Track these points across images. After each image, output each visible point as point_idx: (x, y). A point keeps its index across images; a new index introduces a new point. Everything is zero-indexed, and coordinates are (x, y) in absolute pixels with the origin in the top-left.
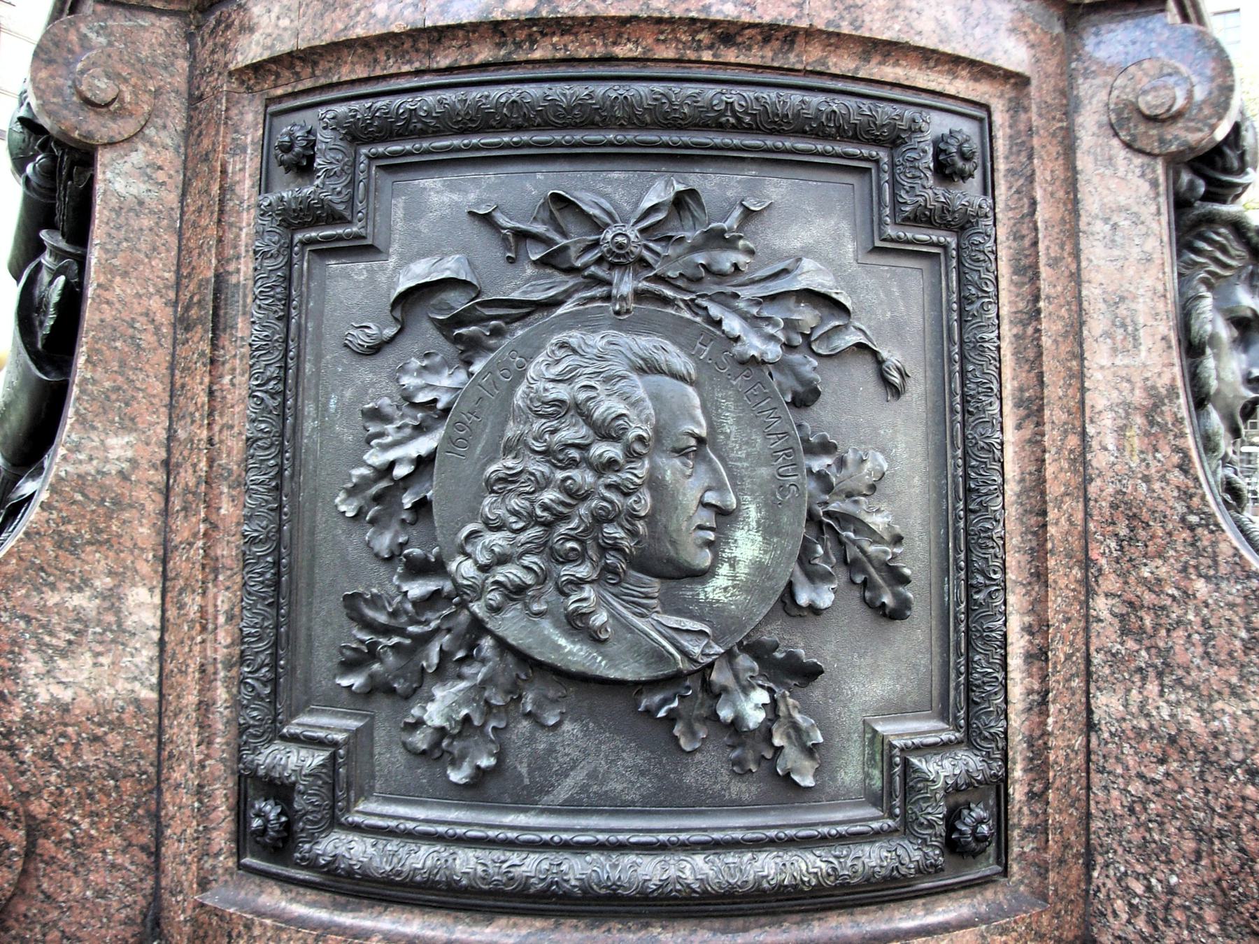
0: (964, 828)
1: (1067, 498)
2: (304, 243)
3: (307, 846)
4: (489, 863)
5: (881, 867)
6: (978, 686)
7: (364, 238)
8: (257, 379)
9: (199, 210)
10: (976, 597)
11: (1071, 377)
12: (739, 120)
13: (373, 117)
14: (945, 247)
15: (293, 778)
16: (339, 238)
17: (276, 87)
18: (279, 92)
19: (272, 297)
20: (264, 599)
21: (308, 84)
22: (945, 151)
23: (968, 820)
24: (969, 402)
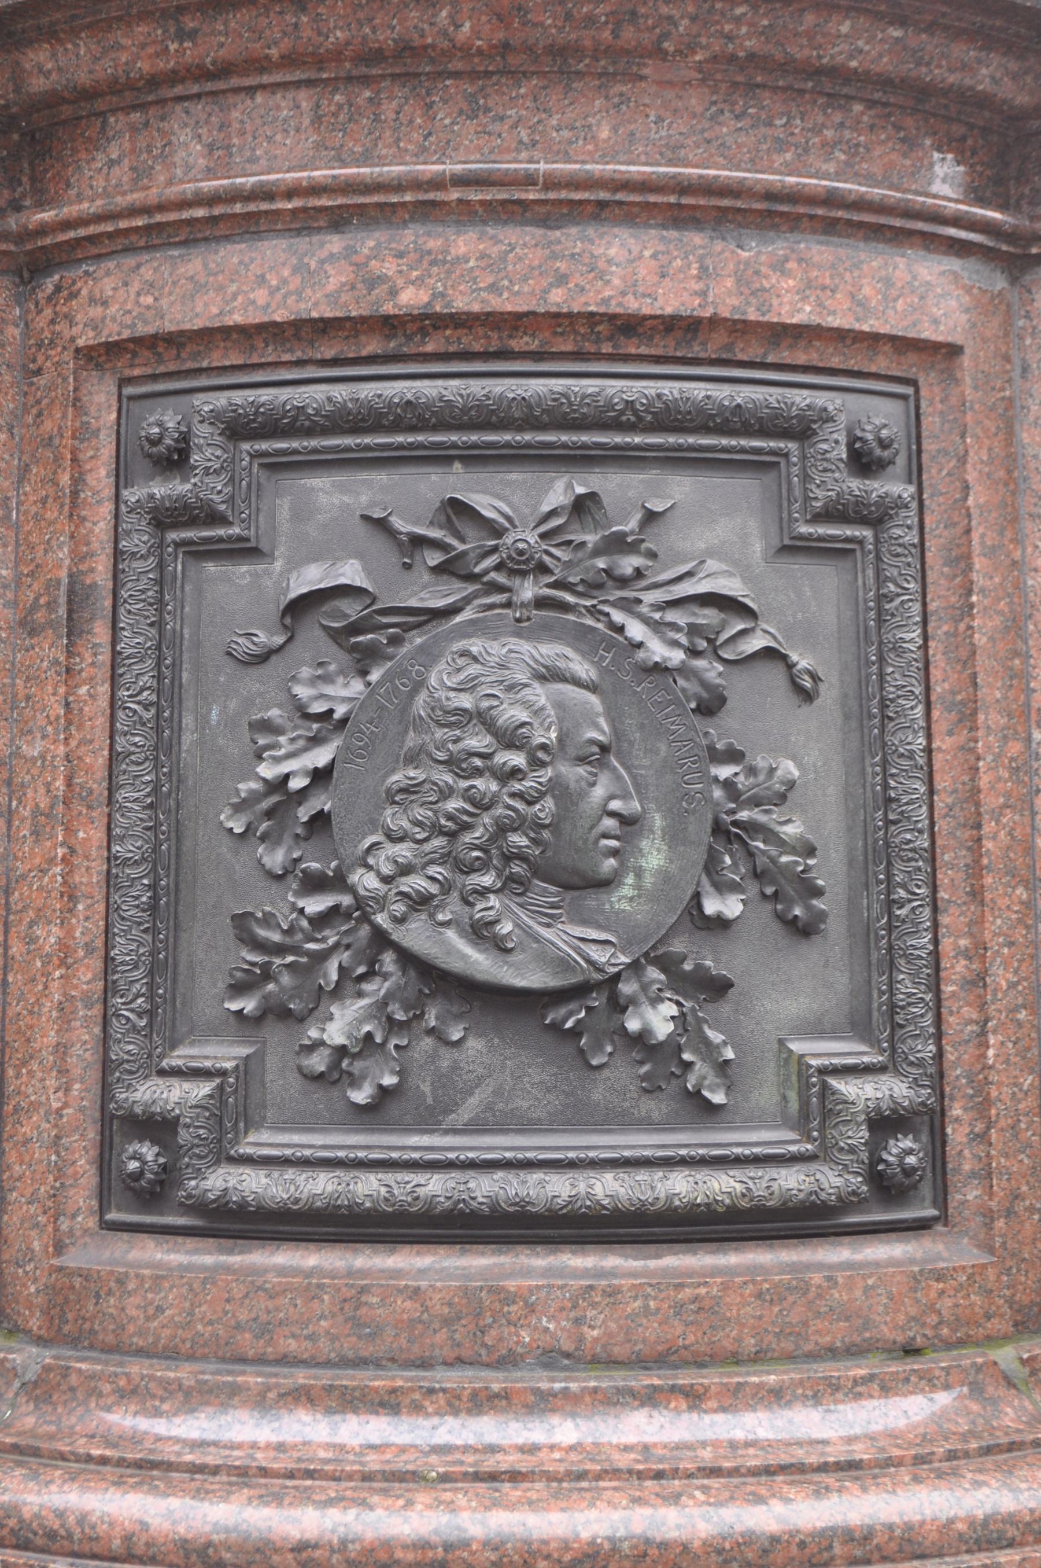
0: (891, 1159)
1: (1008, 811)
2: (177, 545)
3: (193, 1183)
4: (393, 1184)
5: (800, 1191)
6: (902, 1008)
7: (248, 540)
8: (128, 689)
9: (44, 501)
10: (898, 912)
11: (1011, 678)
12: (640, 419)
13: (256, 413)
14: (861, 542)
15: (177, 1111)
16: (220, 540)
17: (132, 366)
18: (136, 372)
19: (144, 601)
20: (140, 924)
21: (172, 367)
22: (861, 439)
23: (894, 1151)
24: (888, 706)
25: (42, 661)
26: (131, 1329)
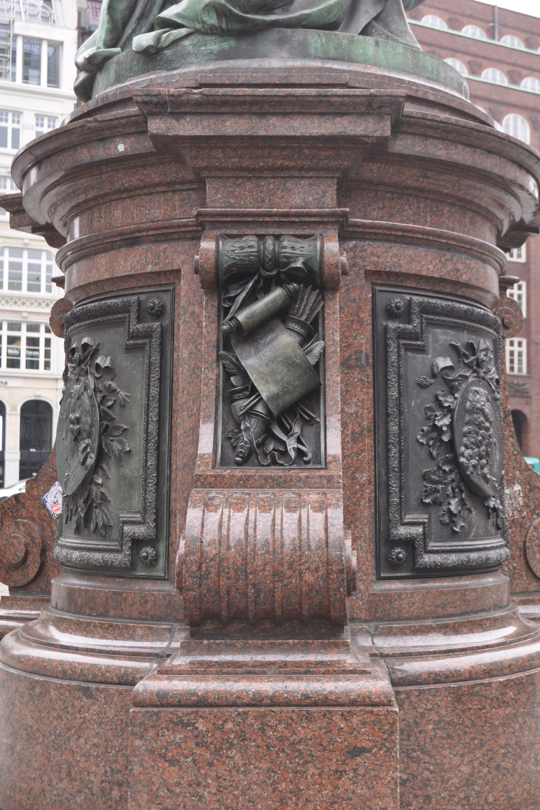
9: (352, 322)
16: (414, 345)
17: (378, 279)
18: (379, 282)
21: (393, 283)
25: (354, 378)
26: (404, 611)
